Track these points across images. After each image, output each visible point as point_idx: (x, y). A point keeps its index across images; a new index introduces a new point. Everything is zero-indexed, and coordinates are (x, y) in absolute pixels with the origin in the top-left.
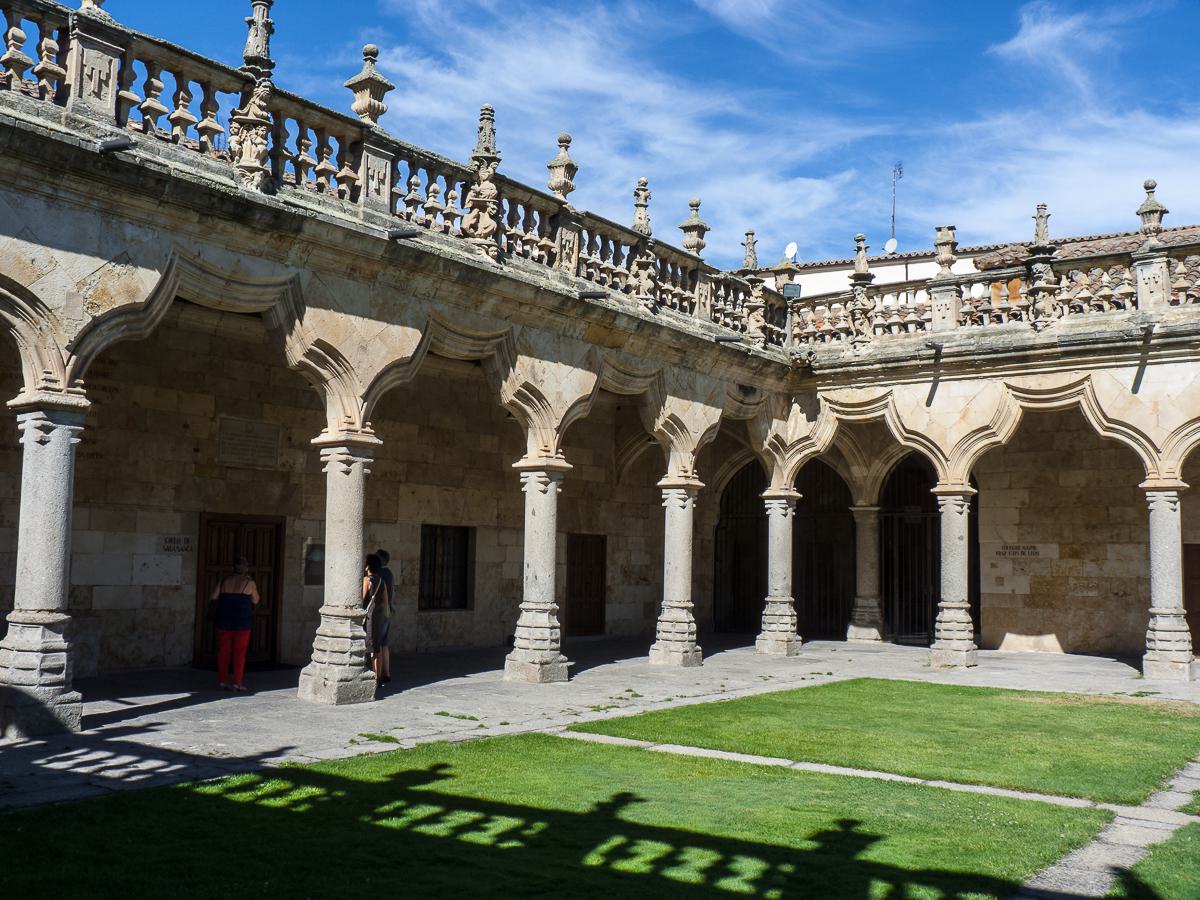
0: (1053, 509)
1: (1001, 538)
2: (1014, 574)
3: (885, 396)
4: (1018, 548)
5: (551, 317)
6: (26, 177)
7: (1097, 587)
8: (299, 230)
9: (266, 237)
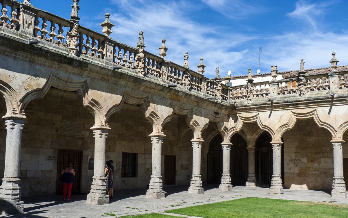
0: (305, 148)
1: (290, 156)
2: (294, 167)
3: (257, 115)
4: (295, 159)
5: (160, 92)
6: (8, 52)
7: (318, 171)
8: (87, 67)
9: (77, 69)
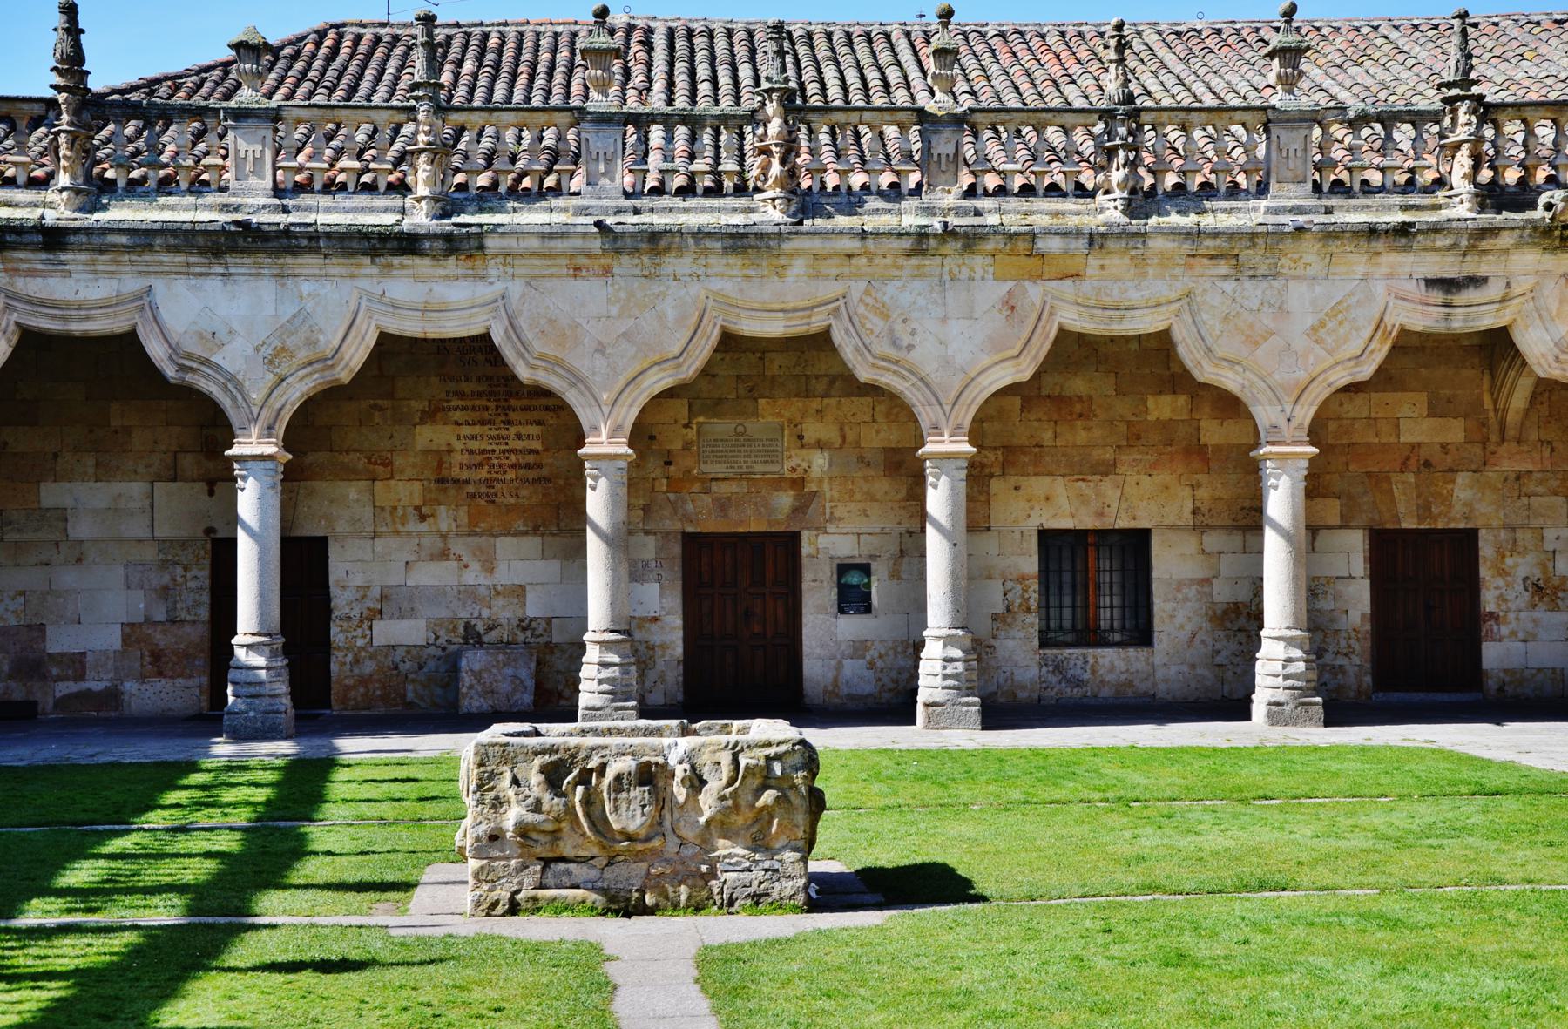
8: (481, 247)
